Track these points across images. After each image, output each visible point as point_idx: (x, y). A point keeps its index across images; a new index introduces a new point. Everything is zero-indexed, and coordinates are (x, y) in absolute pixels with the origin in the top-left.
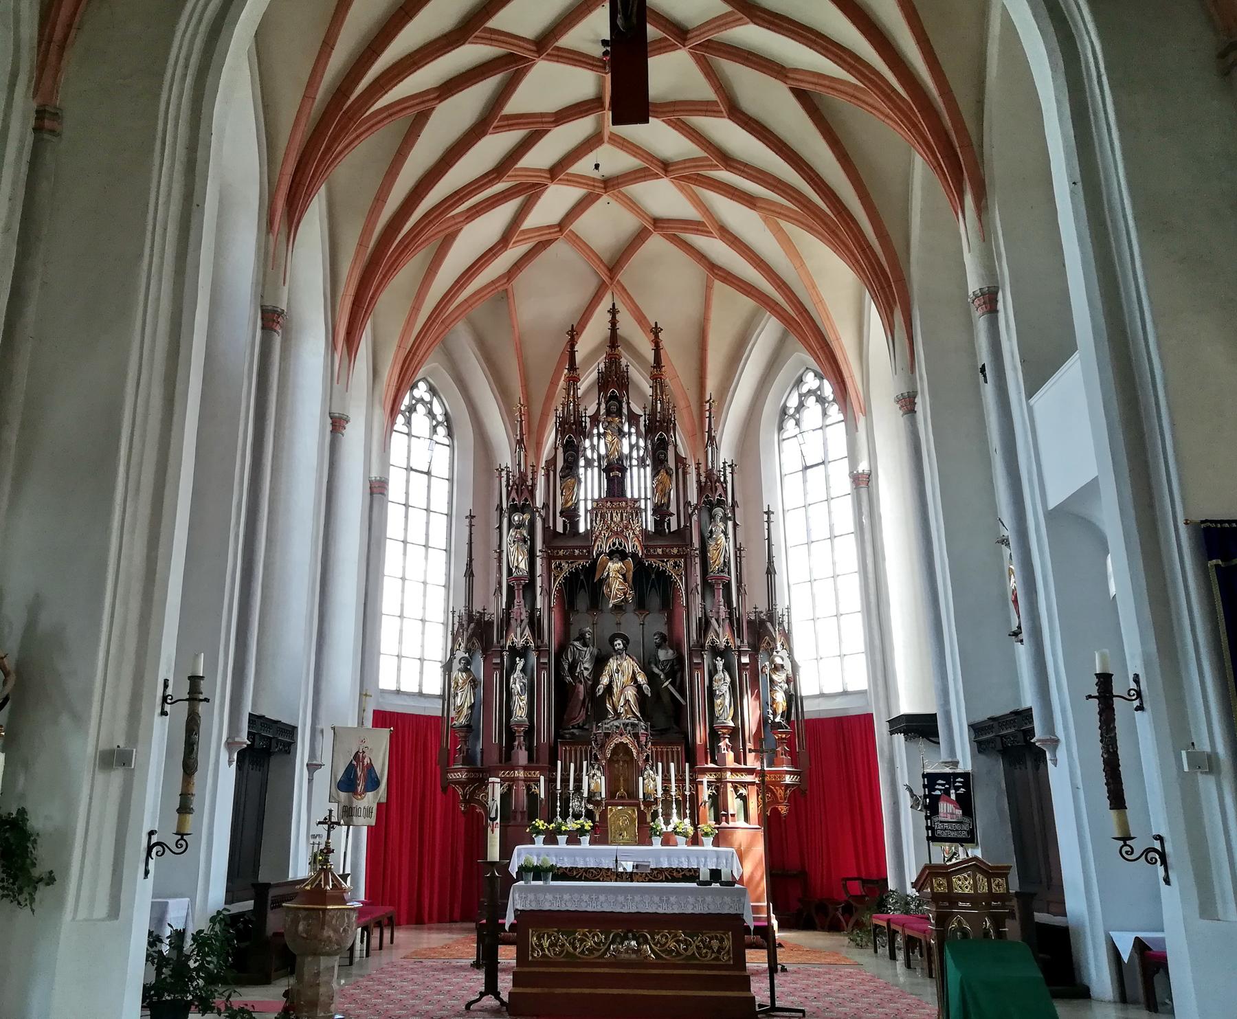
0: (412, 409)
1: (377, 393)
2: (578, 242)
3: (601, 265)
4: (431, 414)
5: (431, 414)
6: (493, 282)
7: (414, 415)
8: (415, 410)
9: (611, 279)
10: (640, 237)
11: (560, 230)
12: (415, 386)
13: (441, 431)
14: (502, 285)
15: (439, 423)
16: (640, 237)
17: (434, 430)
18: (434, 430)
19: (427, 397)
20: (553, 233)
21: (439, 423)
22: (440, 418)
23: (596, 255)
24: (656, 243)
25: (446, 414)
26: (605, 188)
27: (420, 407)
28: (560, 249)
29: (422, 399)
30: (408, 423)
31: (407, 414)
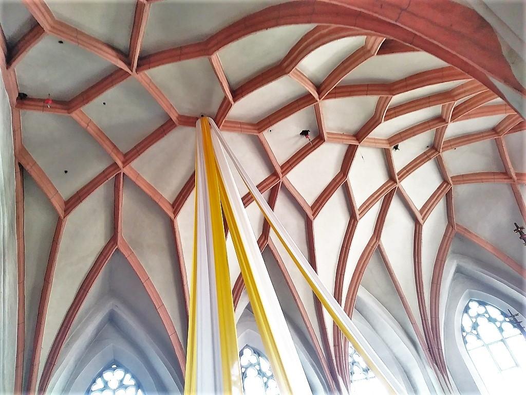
0: (475, 326)
1: (422, 356)
2: (462, 179)
3: (496, 177)
4: (490, 319)
5: (490, 319)
6: (445, 236)
7: (479, 328)
8: (478, 325)
9: (511, 178)
10: (498, 145)
11: (448, 184)
12: (467, 309)
13: (508, 327)
14: (451, 233)
15: (501, 323)
16: (498, 145)
17: (501, 329)
18: (501, 329)
19: (482, 310)
20: (444, 189)
21: (501, 323)
22: (501, 318)
23: (487, 174)
24: (511, 140)
25: (503, 313)
26: (436, 150)
27: (481, 320)
28: (461, 191)
29: (479, 315)
30: (478, 335)
31: (475, 332)
